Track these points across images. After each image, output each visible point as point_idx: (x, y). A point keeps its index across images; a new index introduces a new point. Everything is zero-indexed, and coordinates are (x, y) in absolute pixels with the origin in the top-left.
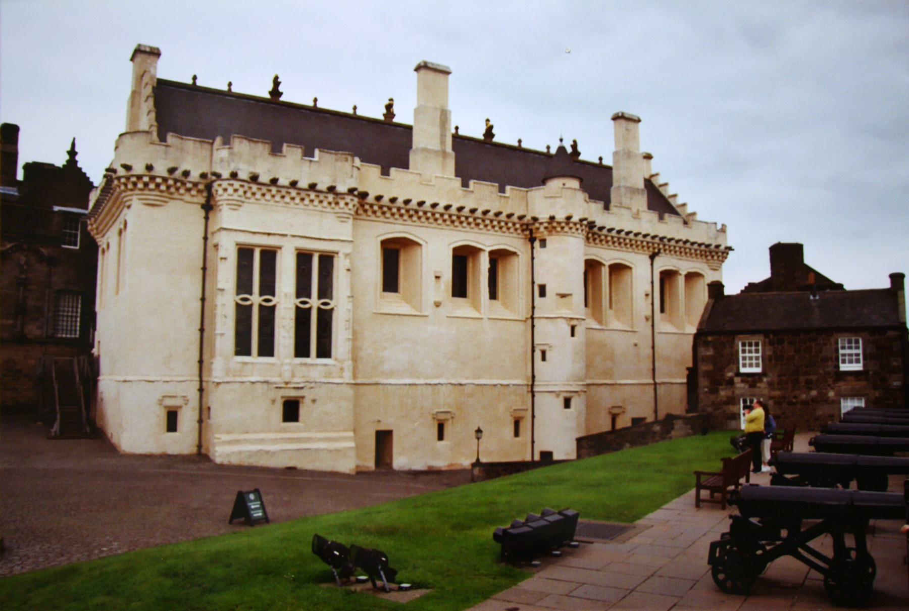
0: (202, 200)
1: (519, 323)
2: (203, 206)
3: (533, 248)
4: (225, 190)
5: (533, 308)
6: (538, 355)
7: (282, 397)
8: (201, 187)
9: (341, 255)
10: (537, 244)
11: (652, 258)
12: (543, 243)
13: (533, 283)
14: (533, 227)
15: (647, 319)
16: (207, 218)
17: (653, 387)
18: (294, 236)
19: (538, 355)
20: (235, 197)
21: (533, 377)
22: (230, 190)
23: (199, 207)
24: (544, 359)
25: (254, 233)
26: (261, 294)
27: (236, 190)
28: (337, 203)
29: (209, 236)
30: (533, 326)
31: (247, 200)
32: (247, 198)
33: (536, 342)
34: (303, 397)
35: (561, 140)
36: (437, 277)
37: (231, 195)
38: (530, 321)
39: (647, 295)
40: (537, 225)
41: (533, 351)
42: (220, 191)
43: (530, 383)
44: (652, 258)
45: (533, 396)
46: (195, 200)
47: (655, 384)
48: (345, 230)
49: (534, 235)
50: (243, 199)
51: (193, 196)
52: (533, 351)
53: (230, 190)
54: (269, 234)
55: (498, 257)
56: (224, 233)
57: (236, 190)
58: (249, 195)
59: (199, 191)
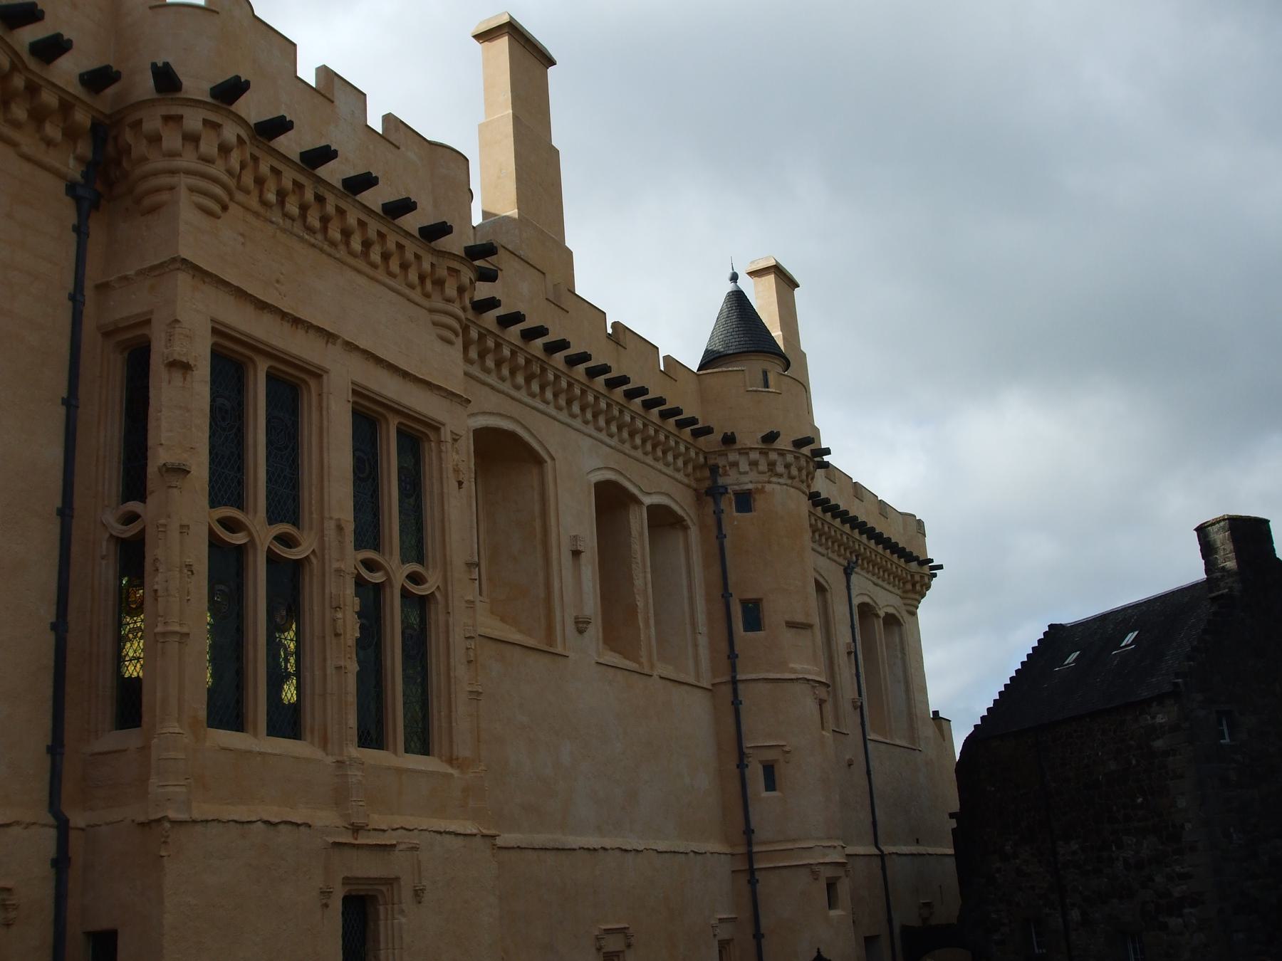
0: (74, 170)
1: (699, 693)
2: (71, 188)
3: (718, 513)
4: (192, 139)
5: (732, 656)
6: (755, 773)
7: (347, 881)
8: (82, 118)
9: (446, 435)
10: (728, 504)
11: (848, 572)
12: (745, 501)
13: (726, 595)
14: (721, 462)
15: (855, 708)
16: (81, 231)
17: (878, 862)
18: (350, 347)
19: (755, 773)
20: (217, 170)
21: (749, 832)
22: (209, 146)
23: (61, 186)
24: (771, 784)
25: (262, 306)
26: (272, 519)
27: (224, 149)
28: (439, 283)
29: (89, 292)
30: (736, 703)
31: (240, 196)
32: (240, 188)
33: (747, 744)
34: (392, 882)
35: (734, 278)
36: (576, 554)
37: (207, 160)
38: (727, 690)
39: (849, 653)
40: (733, 457)
41: (742, 766)
42: (172, 140)
43: (741, 850)
44: (848, 572)
45: (753, 882)
46: (52, 158)
47: (882, 856)
48: (445, 362)
49: (721, 481)
50: (232, 183)
51: (49, 143)
52: (742, 766)
53: (209, 146)
54: (296, 321)
55: (662, 520)
56: (183, 280)
57: (224, 149)
58: (248, 179)
59: (71, 134)
